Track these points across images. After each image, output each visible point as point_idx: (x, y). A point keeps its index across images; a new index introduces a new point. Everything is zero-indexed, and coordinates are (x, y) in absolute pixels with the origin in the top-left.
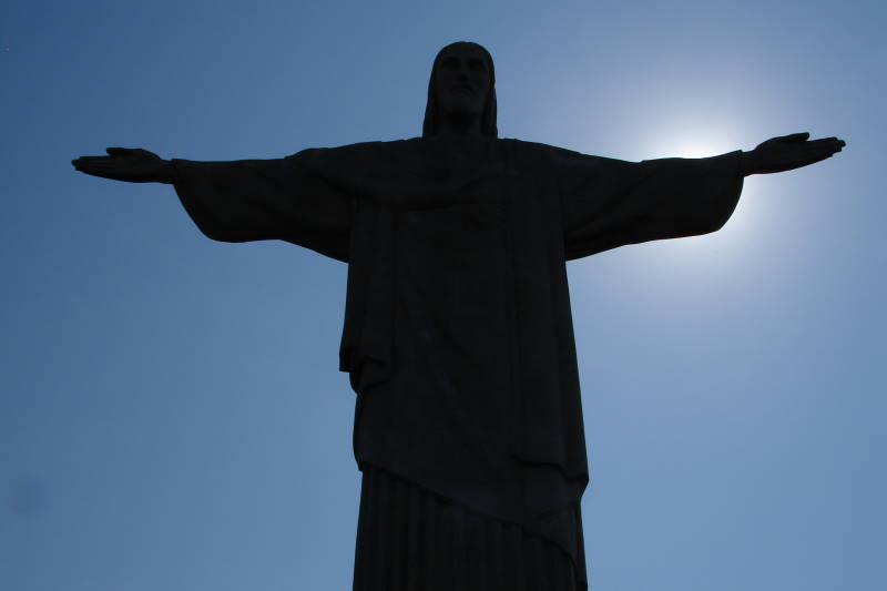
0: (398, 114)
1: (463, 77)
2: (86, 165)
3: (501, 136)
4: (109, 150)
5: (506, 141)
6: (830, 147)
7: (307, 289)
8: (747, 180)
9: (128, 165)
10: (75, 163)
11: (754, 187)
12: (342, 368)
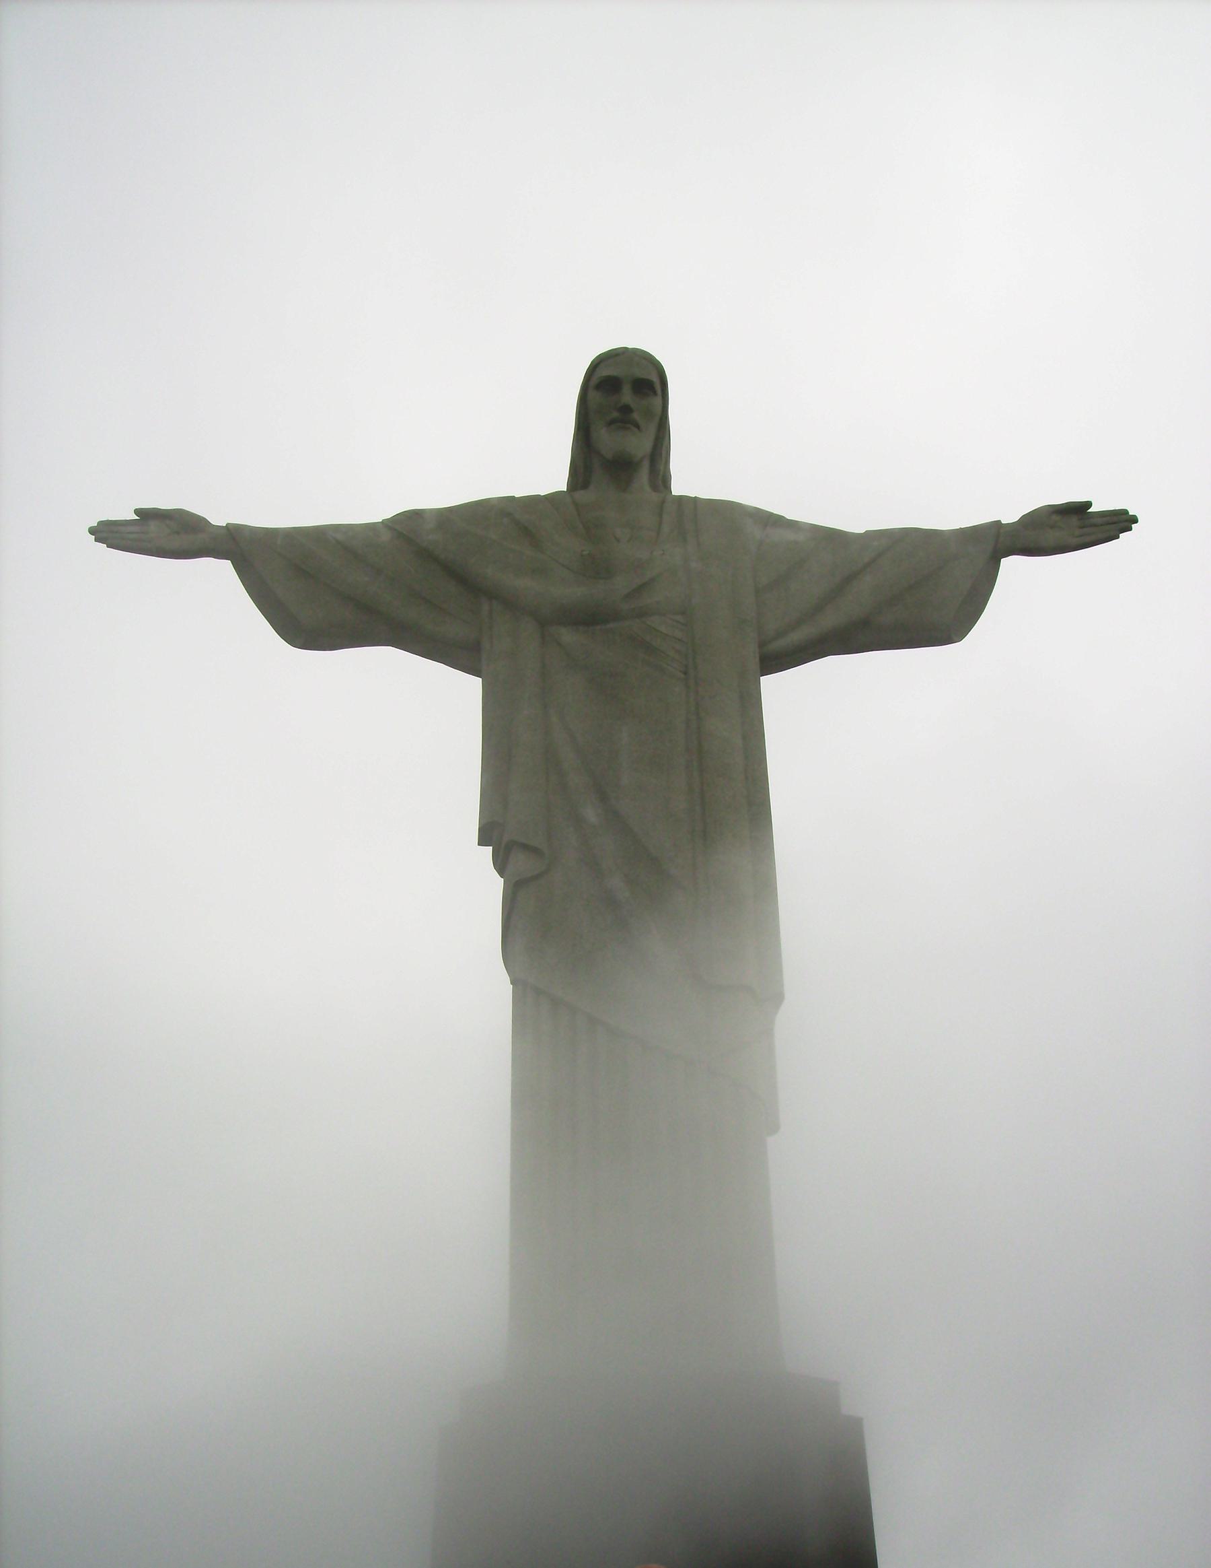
0: (536, 460)
1: (623, 401)
2: (109, 534)
3: (679, 487)
4: (137, 512)
5: (681, 499)
6: (1118, 523)
7: (421, 717)
8: (1005, 562)
9: (164, 534)
10: (92, 531)
12: (482, 842)
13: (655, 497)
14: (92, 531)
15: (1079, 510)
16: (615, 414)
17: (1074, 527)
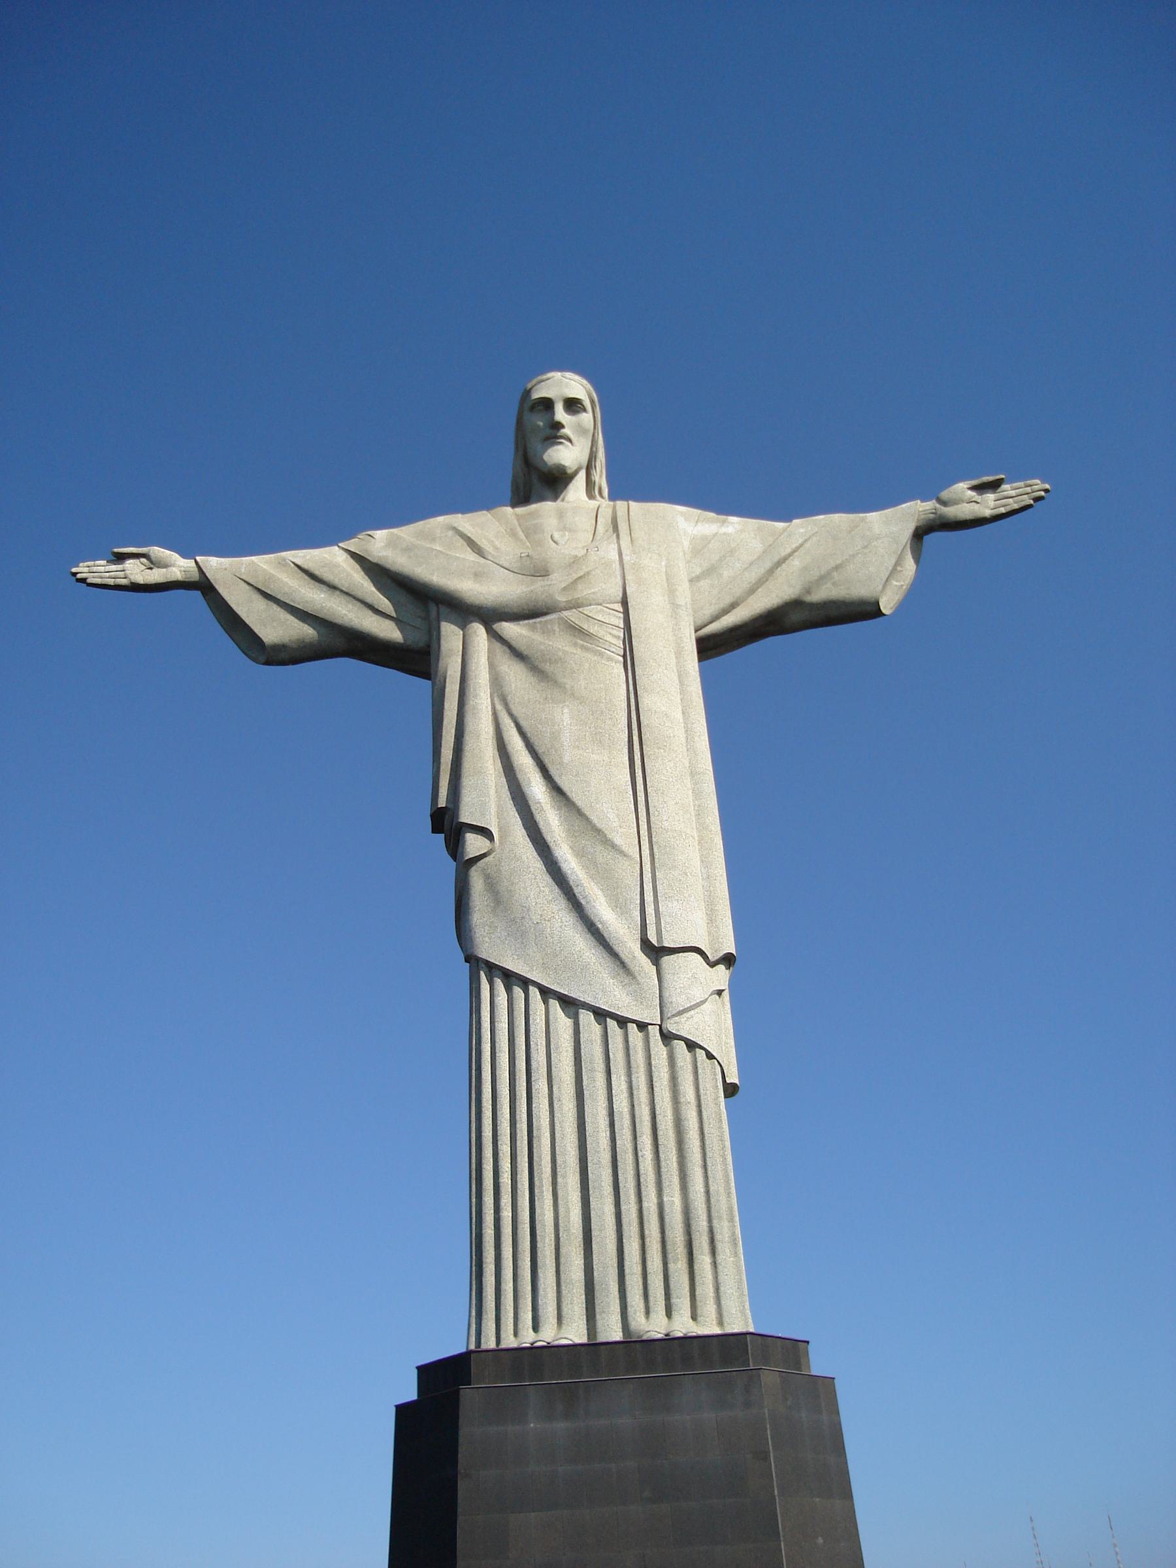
8: (927, 538)
13: (593, 504)
16: (549, 432)
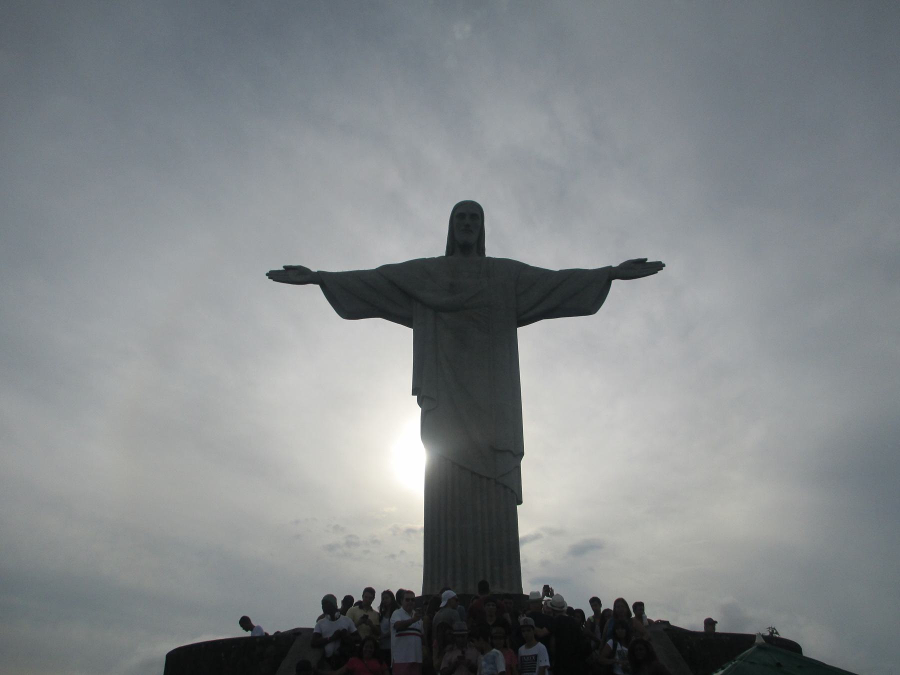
1: (467, 222)
2: (274, 276)
3: (489, 253)
5: (489, 258)
6: (658, 267)
7: (390, 346)
8: (614, 282)
10: (267, 275)
11: (616, 284)
14: (267, 275)
15: (642, 262)
17: (637, 269)
